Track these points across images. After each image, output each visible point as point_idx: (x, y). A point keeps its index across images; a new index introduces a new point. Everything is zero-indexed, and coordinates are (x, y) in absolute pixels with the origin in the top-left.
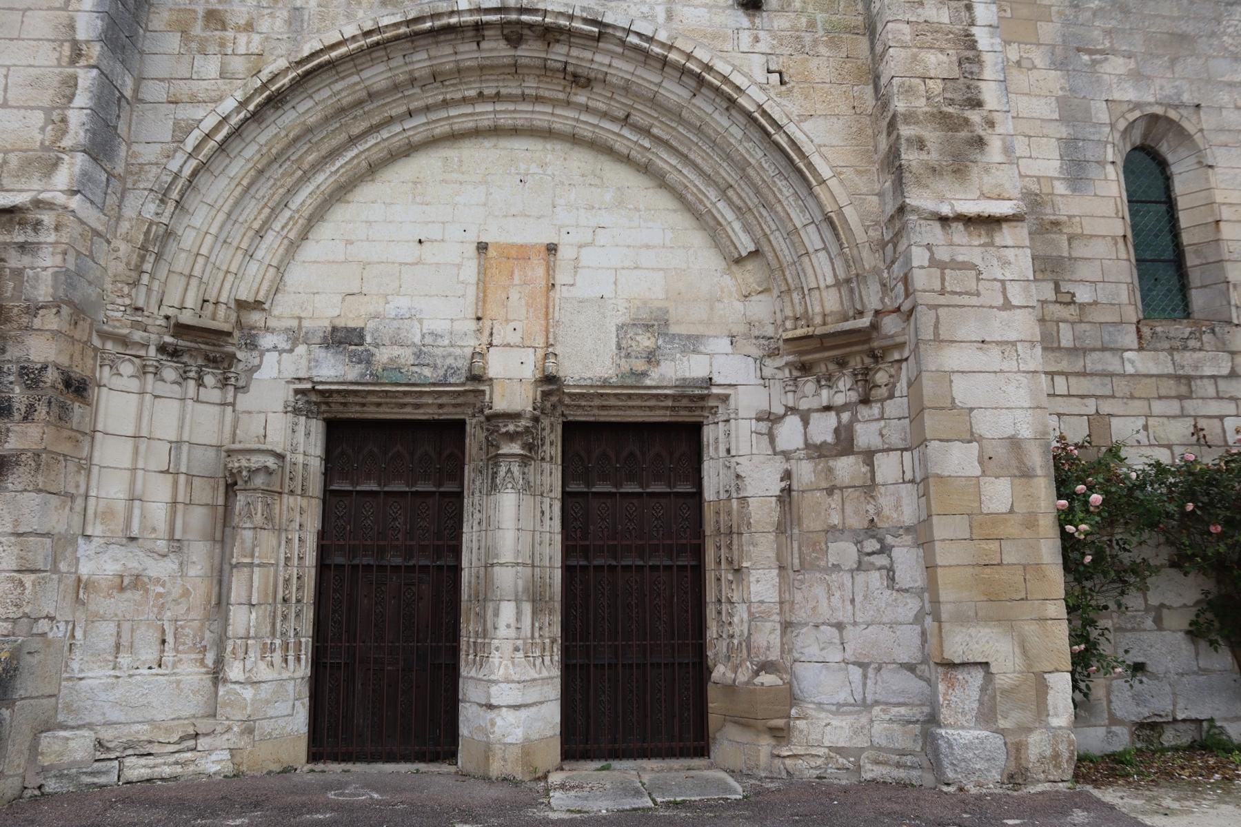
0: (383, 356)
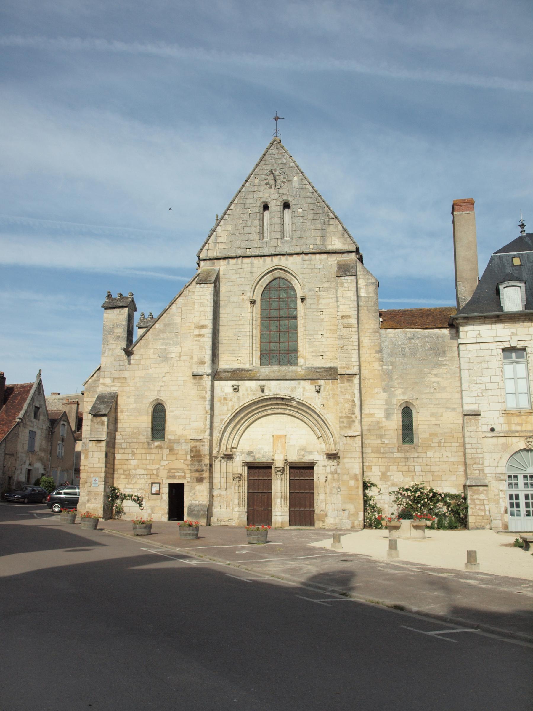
0: (257, 456)
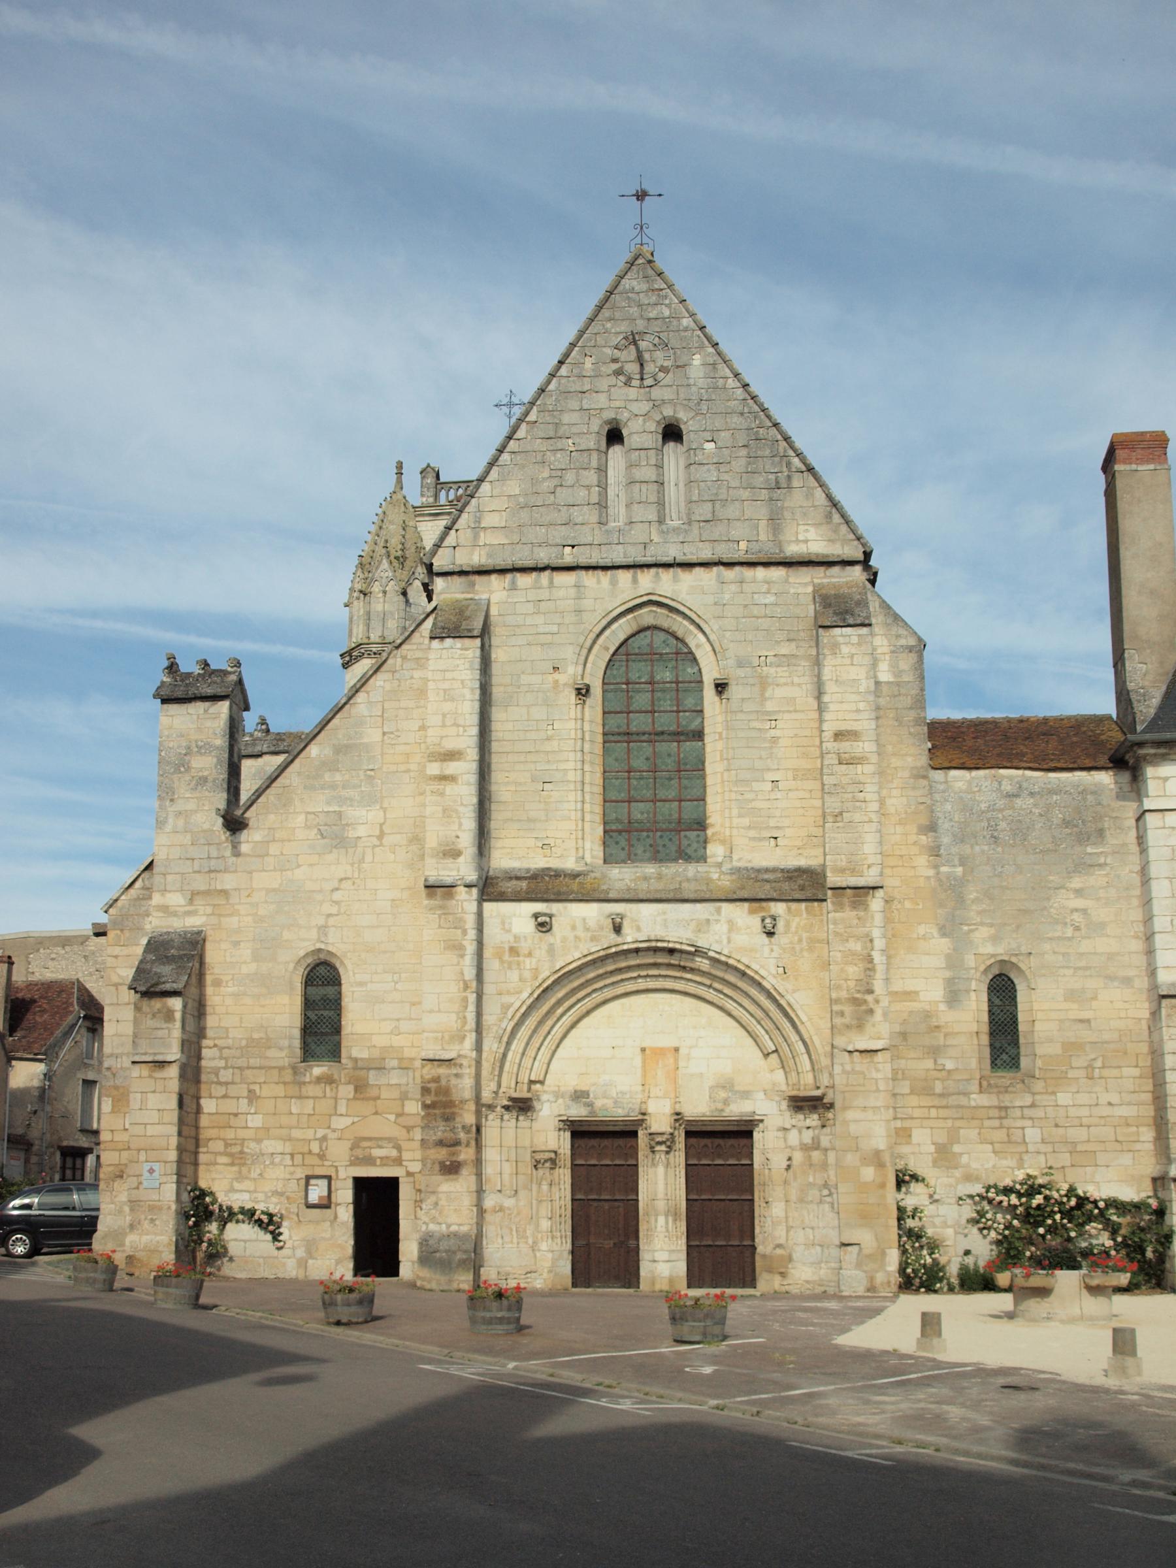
0: (599, 1103)
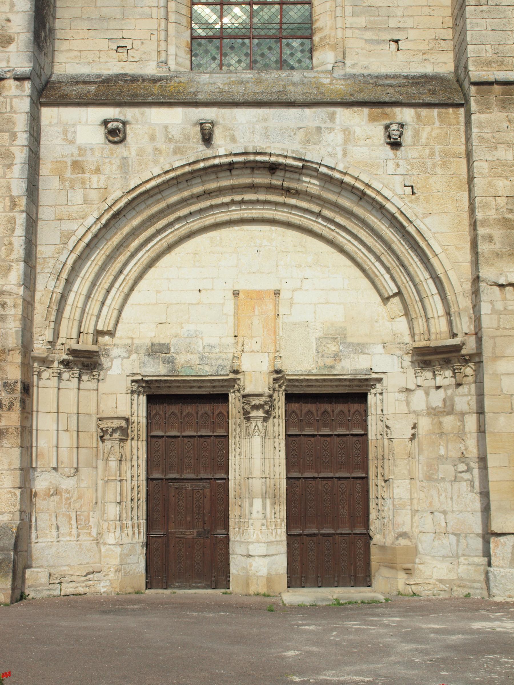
0: (181, 359)
